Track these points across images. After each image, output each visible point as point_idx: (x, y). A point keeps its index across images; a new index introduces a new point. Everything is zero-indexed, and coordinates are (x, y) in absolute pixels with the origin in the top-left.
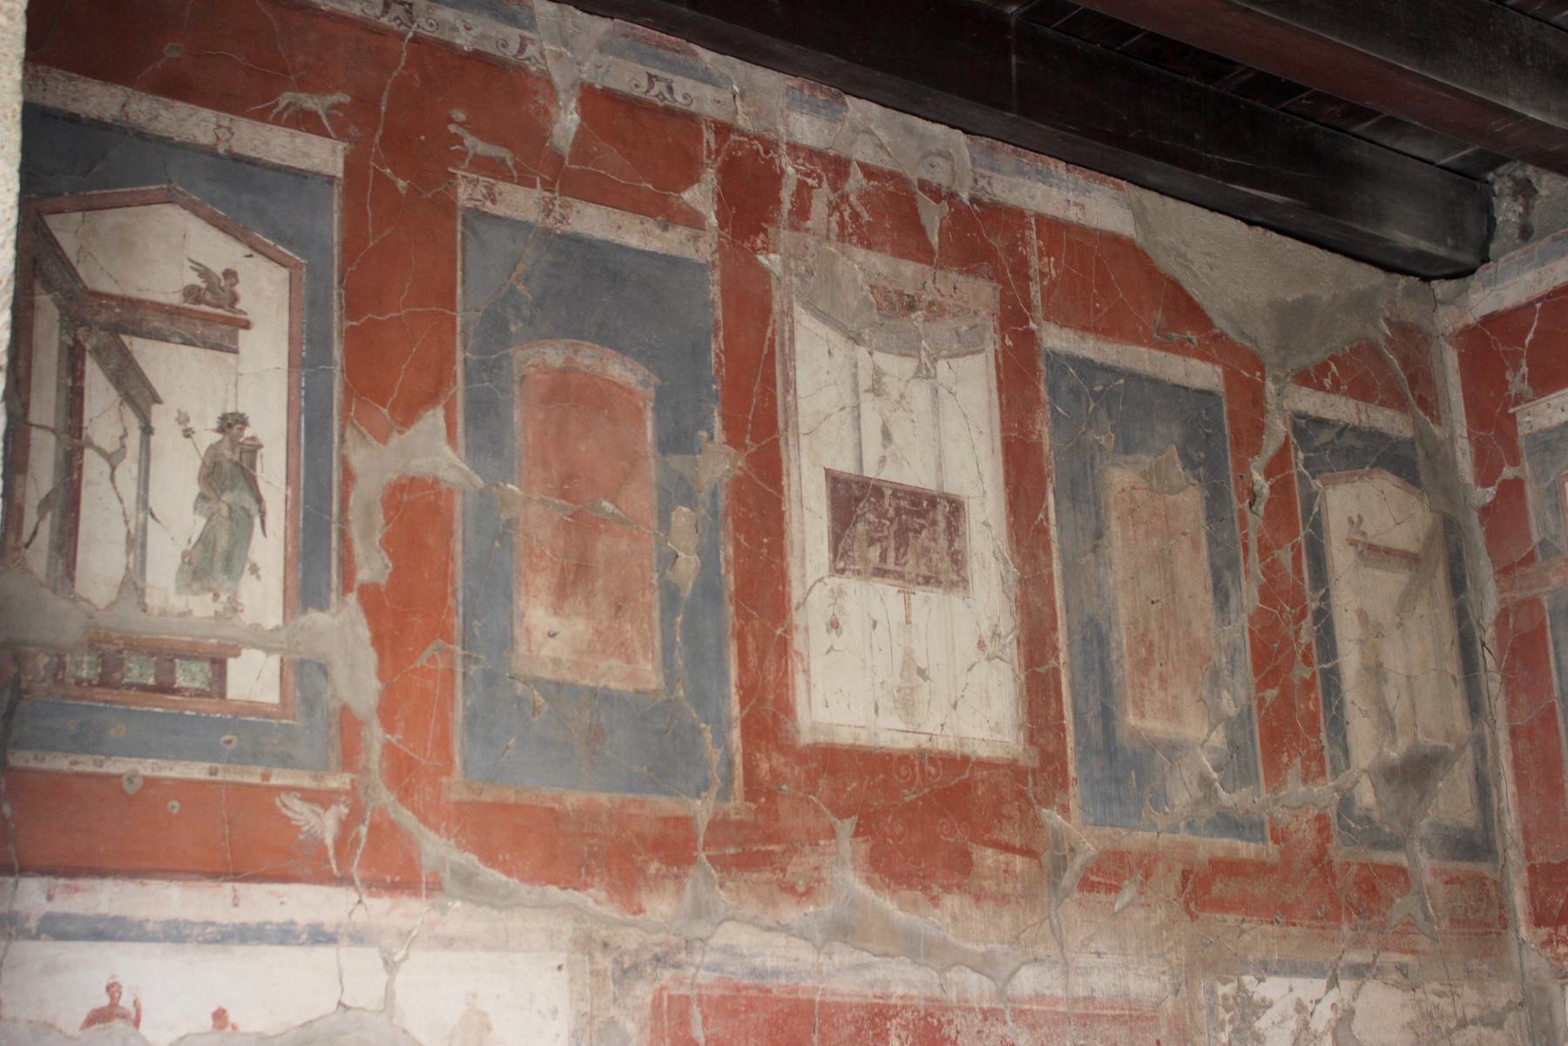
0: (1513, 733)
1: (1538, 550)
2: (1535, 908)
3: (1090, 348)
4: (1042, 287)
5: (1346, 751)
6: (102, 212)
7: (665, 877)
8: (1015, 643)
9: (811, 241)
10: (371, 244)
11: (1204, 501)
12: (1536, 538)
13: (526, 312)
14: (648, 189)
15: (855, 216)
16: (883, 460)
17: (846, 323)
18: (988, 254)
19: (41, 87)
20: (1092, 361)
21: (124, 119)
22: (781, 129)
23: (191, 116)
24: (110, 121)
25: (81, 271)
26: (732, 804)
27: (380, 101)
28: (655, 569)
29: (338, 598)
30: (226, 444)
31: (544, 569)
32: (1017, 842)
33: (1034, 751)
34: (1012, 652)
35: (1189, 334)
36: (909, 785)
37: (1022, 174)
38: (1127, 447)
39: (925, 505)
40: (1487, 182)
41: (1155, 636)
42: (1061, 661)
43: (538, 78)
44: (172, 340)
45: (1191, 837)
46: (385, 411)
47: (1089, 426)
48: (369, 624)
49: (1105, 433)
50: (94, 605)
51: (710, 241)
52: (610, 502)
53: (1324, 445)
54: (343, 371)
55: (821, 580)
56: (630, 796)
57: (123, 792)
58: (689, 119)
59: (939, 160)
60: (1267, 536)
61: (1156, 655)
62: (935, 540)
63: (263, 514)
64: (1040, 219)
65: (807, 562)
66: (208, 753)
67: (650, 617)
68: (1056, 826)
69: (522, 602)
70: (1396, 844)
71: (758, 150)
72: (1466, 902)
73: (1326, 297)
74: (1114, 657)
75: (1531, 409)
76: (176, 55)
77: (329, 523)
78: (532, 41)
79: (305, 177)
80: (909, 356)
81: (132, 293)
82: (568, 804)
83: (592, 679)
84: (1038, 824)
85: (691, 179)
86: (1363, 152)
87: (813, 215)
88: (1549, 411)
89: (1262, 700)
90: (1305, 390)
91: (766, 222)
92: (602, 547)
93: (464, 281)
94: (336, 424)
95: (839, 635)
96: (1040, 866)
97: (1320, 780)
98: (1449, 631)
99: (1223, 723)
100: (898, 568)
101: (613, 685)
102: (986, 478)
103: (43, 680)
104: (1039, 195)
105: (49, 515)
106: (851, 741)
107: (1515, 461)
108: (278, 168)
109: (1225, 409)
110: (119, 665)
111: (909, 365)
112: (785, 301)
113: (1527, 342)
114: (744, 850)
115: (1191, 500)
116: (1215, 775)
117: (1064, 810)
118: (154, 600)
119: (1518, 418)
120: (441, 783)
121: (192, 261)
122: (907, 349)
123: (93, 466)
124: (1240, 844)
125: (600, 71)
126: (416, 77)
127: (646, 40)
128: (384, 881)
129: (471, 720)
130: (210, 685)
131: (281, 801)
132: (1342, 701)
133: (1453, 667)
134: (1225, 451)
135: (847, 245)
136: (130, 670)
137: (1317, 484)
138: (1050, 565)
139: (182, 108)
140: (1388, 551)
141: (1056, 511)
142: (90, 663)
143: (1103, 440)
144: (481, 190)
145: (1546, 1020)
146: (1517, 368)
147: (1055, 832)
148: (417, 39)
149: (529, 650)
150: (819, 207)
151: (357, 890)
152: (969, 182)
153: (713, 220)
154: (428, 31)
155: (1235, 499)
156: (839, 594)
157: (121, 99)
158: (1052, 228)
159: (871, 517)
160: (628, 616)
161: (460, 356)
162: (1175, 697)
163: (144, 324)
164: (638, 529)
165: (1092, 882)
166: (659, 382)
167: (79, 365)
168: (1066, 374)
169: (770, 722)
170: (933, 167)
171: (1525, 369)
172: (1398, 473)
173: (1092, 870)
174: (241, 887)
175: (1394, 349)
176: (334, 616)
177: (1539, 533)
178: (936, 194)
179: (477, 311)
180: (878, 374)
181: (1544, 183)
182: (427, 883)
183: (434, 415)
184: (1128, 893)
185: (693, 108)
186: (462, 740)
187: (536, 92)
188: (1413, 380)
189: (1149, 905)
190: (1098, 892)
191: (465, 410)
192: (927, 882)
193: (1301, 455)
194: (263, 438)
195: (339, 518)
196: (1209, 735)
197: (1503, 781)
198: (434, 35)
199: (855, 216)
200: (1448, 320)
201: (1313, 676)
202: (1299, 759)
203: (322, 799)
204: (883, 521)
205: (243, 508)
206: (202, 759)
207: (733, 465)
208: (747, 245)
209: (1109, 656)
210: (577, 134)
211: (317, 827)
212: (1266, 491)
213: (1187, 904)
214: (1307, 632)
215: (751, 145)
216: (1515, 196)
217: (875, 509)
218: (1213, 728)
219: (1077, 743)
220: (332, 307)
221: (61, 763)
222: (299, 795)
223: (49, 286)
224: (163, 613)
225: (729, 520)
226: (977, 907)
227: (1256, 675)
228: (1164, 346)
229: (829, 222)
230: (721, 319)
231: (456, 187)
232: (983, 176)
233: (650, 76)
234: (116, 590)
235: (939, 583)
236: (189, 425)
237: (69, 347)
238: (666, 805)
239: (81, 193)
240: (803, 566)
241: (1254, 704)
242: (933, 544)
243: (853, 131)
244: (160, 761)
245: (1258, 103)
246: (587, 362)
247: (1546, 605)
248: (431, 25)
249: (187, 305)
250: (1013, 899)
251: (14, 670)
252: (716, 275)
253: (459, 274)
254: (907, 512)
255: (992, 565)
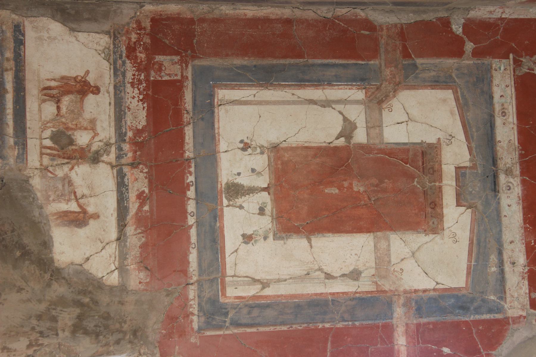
0: (288, 22)
1: (411, 62)
2: (165, 20)
12: (419, 61)
75: (508, 71)
88: (503, 86)
107: (476, 53)
119: (504, 61)
145: (86, 15)
177: (422, 64)
247: (372, 62)
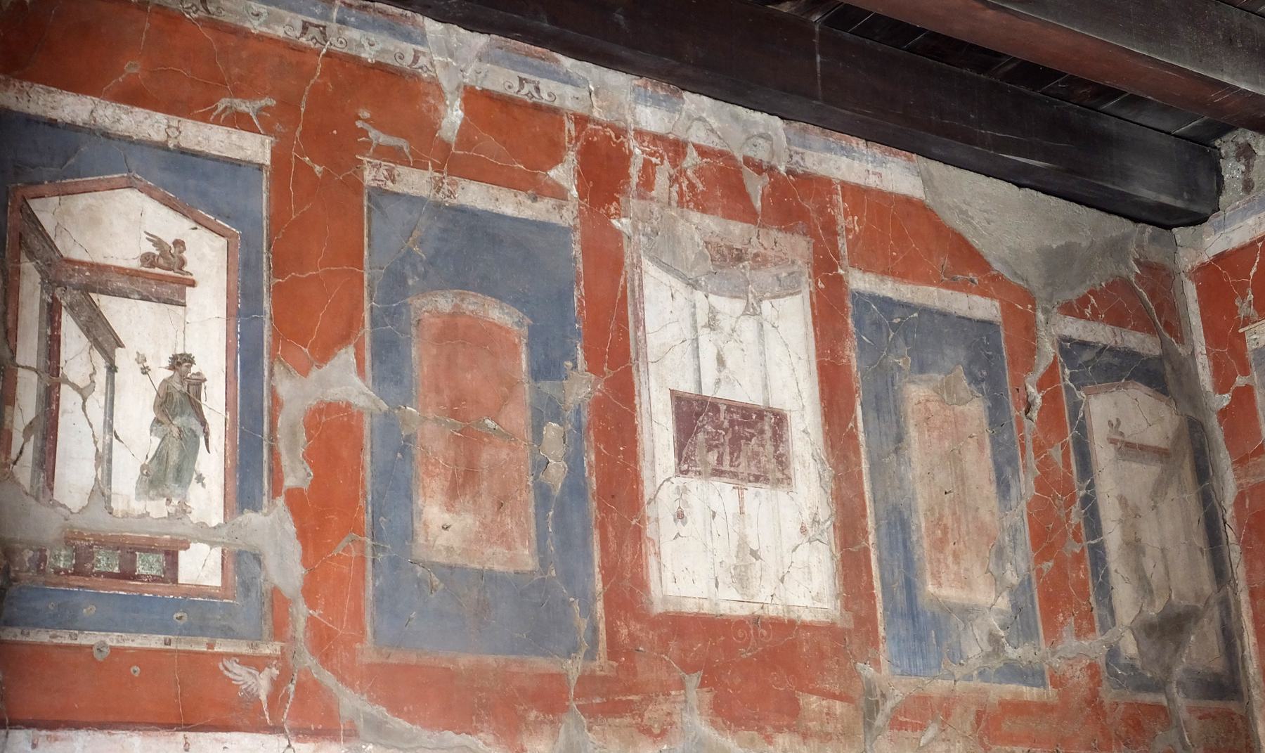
0: (1253, 594)
3: (889, 288)
4: (848, 241)
5: (1112, 612)
6: (75, 196)
7: (542, 722)
8: (832, 527)
9: (655, 208)
10: (294, 217)
11: (987, 410)
13: (421, 269)
14: (521, 169)
15: (692, 186)
16: (718, 382)
17: (685, 272)
18: (802, 214)
19: (26, 99)
20: (891, 299)
21: (93, 122)
22: (630, 119)
23: (146, 119)
24: (81, 124)
25: (58, 243)
26: (597, 663)
27: (300, 103)
28: (530, 473)
29: (269, 501)
30: (177, 379)
31: (438, 475)
32: (837, 690)
33: (849, 615)
34: (829, 535)
35: (971, 276)
36: (746, 645)
37: (829, 150)
38: (922, 368)
39: (754, 417)
40: (1215, 148)
41: (948, 520)
42: (871, 542)
43: (430, 83)
44: (132, 296)
45: (983, 683)
46: (306, 350)
47: (889, 351)
48: (294, 521)
49: (903, 357)
50: (69, 509)
51: (572, 209)
52: (492, 420)
53: (1087, 363)
54: (271, 319)
55: (668, 480)
56: (513, 657)
57: (94, 659)
58: (554, 112)
59: (761, 141)
60: (1041, 436)
61: (949, 536)
62: (763, 446)
63: (207, 434)
64: (844, 185)
65: (657, 467)
66: (164, 628)
67: (526, 512)
68: (869, 677)
69: (420, 502)
70: (1159, 686)
71: (610, 135)
72: (1217, 733)
73: (1085, 244)
74: (914, 538)
76: (135, 71)
77: (262, 441)
78: (424, 54)
79: (240, 165)
80: (739, 297)
81: (99, 259)
82: (460, 664)
83: (479, 563)
84: (854, 674)
85: (556, 160)
86: (1111, 125)
87: (656, 187)
89: (1040, 571)
90: (1069, 318)
91: (618, 193)
92: (486, 456)
93: (369, 246)
94: (266, 362)
95: (684, 524)
96: (856, 709)
97: (1090, 636)
98: (1196, 513)
99: (1008, 590)
100: (732, 469)
101: (497, 568)
102: (805, 395)
103: (28, 570)
104: (843, 167)
105: (32, 438)
106: (696, 610)
107: (1245, 371)
108: (217, 159)
109: (1003, 335)
110: (91, 557)
111: (739, 305)
112: (635, 255)
113: (1252, 274)
114: (608, 699)
115: (975, 410)
116: (1002, 633)
117: (876, 663)
118: (118, 505)
120: (355, 649)
121: (148, 234)
122: (737, 293)
123: (68, 399)
124: (1025, 689)
125: (480, 76)
126: (329, 84)
127: (516, 51)
128: (310, 729)
129: (379, 599)
130: (164, 573)
131: (224, 665)
132: (1107, 571)
133: (1200, 541)
134: (1003, 370)
135: (685, 209)
136: (99, 561)
137: (1081, 395)
138: (859, 464)
139: (140, 113)
140: (1143, 448)
141: (865, 422)
142: (65, 556)
143: (901, 362)
144: (383, 172)
146: (1244, 296)
147: (869, 682)
148: (329, 54)
149: (427, 540)
150: (661, 180)
151: (286, 736)
152: (785, 157)
153: (575, 193)
154: (338, 47)
155: (1013, 408)
156: (683, 491)
157: (90, 107)
158: (856, 193)
159: (709, 428)
160: (508, 512)
161: (367, 306)
162: (966, 570)
163: (109, 284)
164: (516, 440)
165: (901, 721)
166: (531, 322)
167: (57, 318)
168: (870, 310)
169: (628, 596)
170: (755, 146)
171: (1251, 297)
172: (1149, 384)
173: (900, 712)
174: (191, 735)
175: (1143, 284)
176: (266, 515)
178: (758, 168)
179: (381, 268)
180: (713, 314)
181: (1261, 144)
182: (344, 730)
183: (346, 352)
184: (931, 731)
185: (556, 104)
186: (372, 614)
187: (427, 94)
188: (1159, 308)
189: (949, 740)
190: (906, 730)
191: (372, 347)
192: (762, 724)
193: (1067, 371)
194: (206, 376)
195: (269, 437)
196: (996, 600)
197: (1245, 634)
198: (345, 51)
199: (692, 186)
200: (1187, 260)
201: (1083, 549)
202: (1073, 618)
203: (256, 663)
204: (720, 431)
205: (191, 429)
206: (158, 633)
207: (594, 388)
208: (602, 211)
209: (910, 538)
210: (461, 125)
211: (253, 686)
212: (1039, 401)
213: (981, 738)
214: (1076, 515)
215: (604, 132)
216: (1238, 158)
217: (713, 421)
218: (999, 594)
219: (885, 609)
220: (262, 267)
221: (43, 637)
222: (238, 661)
223: (32, 255)
224: (126, 515)
225: (591, 433)
226: (805, 744)
227: (1034, 550)
228: (953, 285)
229: (670, 192)
230: (582, 270)
231: (363, 170)
232: (797, 153)
233: (521, 80)
234: (88, 497)
235: (767, 480)
236: (145, 365)
237: (48, 304)
238: (542, 664)
239: (58, 181)
240: (653, 469)
241: (1034, 574)
242: (761, 449)
243: (689, 119)
244: (123, 634)
245: (1023, 88)
246: (471, 307)
248: (341, 43)
249: (143, 269)
250: (835, 737)
251: (5, 562)
252: (577, 236)
253: (366, 240)
254: (739, 424)
255: (811, 465)
